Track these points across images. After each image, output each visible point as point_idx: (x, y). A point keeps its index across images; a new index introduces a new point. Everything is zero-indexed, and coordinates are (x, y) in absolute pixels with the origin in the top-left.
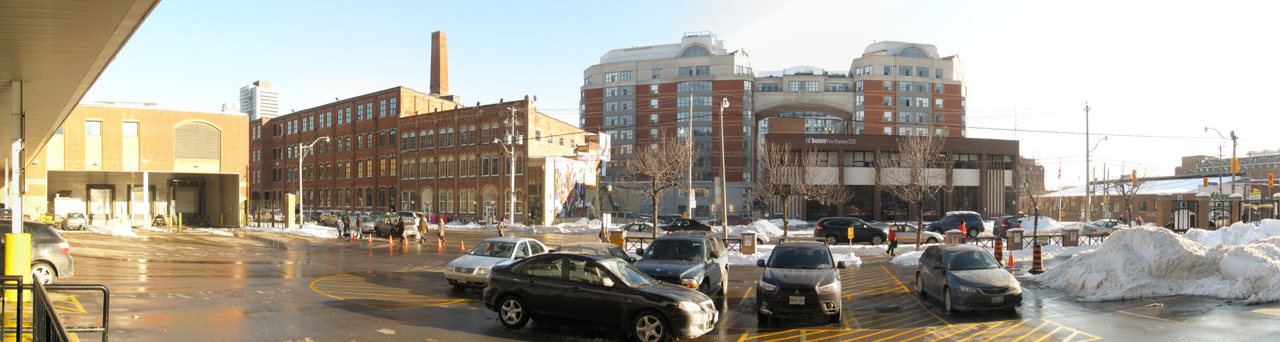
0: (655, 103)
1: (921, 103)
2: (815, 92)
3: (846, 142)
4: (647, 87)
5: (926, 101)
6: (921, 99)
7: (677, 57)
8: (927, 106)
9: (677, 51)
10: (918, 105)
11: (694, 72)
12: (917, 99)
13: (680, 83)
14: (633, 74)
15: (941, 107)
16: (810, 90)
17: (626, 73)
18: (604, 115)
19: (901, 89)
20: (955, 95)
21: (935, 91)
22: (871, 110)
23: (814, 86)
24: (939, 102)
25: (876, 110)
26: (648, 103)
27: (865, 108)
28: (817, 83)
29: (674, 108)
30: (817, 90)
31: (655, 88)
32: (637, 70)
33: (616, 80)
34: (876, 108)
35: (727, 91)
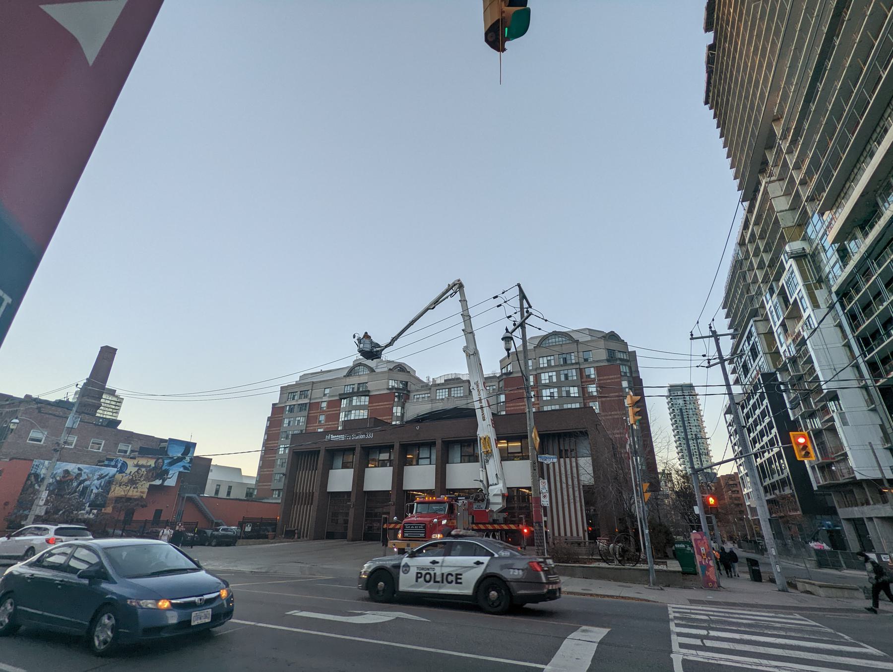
0: (322, 418)
1: (568, 392)
2: (462, 397)
3: (362, 437)
4: (318, 404)
5: (574, 391)
6: (567, 389)
7: (344, 376)
8: (577, 395)
9: (345, 372)
10: (564, 394)
11: (356, 390)
12: (563, 389)
13: (344, 399)
14: (309, 393)
15: (595, 394)
16: (456, 396)
17: (303, 394)
18: (281, 430)
19: (543, 382)
20: (611, 377)
21: (584, 376)
22: (512, 408)
23: (459, 392)
24: (593, 389)
25: (519, 408)
26: (316, 418)
27: (506, 407)
28: (462, 388)
29: (337, 422)
30: (462, 395)
31: (324, 405)
32: (312, 390)
33: (296, 398)
34: (519, 406)
35: (380, 404)
